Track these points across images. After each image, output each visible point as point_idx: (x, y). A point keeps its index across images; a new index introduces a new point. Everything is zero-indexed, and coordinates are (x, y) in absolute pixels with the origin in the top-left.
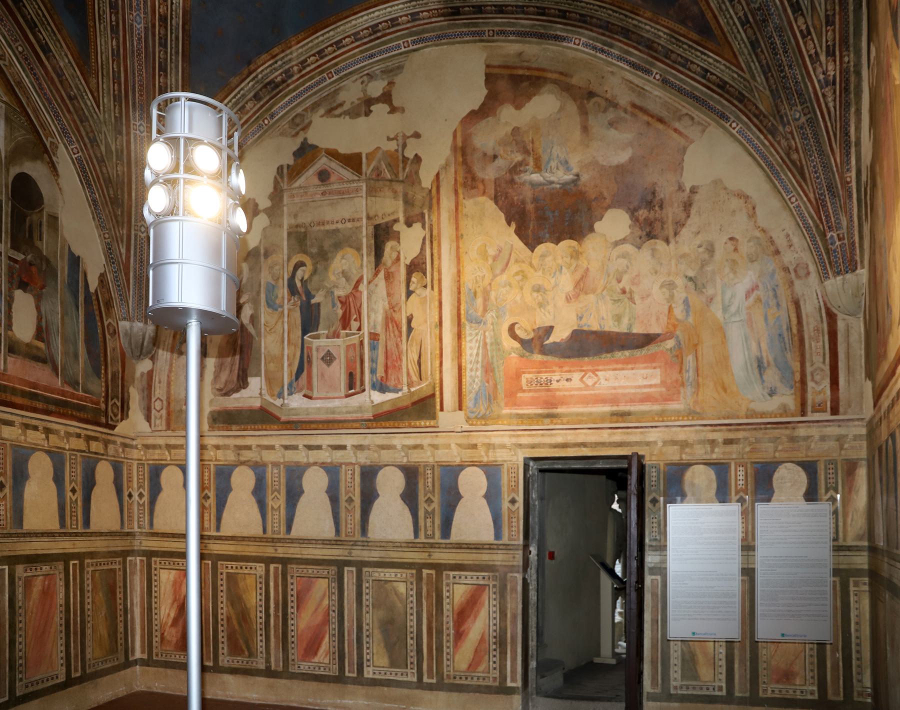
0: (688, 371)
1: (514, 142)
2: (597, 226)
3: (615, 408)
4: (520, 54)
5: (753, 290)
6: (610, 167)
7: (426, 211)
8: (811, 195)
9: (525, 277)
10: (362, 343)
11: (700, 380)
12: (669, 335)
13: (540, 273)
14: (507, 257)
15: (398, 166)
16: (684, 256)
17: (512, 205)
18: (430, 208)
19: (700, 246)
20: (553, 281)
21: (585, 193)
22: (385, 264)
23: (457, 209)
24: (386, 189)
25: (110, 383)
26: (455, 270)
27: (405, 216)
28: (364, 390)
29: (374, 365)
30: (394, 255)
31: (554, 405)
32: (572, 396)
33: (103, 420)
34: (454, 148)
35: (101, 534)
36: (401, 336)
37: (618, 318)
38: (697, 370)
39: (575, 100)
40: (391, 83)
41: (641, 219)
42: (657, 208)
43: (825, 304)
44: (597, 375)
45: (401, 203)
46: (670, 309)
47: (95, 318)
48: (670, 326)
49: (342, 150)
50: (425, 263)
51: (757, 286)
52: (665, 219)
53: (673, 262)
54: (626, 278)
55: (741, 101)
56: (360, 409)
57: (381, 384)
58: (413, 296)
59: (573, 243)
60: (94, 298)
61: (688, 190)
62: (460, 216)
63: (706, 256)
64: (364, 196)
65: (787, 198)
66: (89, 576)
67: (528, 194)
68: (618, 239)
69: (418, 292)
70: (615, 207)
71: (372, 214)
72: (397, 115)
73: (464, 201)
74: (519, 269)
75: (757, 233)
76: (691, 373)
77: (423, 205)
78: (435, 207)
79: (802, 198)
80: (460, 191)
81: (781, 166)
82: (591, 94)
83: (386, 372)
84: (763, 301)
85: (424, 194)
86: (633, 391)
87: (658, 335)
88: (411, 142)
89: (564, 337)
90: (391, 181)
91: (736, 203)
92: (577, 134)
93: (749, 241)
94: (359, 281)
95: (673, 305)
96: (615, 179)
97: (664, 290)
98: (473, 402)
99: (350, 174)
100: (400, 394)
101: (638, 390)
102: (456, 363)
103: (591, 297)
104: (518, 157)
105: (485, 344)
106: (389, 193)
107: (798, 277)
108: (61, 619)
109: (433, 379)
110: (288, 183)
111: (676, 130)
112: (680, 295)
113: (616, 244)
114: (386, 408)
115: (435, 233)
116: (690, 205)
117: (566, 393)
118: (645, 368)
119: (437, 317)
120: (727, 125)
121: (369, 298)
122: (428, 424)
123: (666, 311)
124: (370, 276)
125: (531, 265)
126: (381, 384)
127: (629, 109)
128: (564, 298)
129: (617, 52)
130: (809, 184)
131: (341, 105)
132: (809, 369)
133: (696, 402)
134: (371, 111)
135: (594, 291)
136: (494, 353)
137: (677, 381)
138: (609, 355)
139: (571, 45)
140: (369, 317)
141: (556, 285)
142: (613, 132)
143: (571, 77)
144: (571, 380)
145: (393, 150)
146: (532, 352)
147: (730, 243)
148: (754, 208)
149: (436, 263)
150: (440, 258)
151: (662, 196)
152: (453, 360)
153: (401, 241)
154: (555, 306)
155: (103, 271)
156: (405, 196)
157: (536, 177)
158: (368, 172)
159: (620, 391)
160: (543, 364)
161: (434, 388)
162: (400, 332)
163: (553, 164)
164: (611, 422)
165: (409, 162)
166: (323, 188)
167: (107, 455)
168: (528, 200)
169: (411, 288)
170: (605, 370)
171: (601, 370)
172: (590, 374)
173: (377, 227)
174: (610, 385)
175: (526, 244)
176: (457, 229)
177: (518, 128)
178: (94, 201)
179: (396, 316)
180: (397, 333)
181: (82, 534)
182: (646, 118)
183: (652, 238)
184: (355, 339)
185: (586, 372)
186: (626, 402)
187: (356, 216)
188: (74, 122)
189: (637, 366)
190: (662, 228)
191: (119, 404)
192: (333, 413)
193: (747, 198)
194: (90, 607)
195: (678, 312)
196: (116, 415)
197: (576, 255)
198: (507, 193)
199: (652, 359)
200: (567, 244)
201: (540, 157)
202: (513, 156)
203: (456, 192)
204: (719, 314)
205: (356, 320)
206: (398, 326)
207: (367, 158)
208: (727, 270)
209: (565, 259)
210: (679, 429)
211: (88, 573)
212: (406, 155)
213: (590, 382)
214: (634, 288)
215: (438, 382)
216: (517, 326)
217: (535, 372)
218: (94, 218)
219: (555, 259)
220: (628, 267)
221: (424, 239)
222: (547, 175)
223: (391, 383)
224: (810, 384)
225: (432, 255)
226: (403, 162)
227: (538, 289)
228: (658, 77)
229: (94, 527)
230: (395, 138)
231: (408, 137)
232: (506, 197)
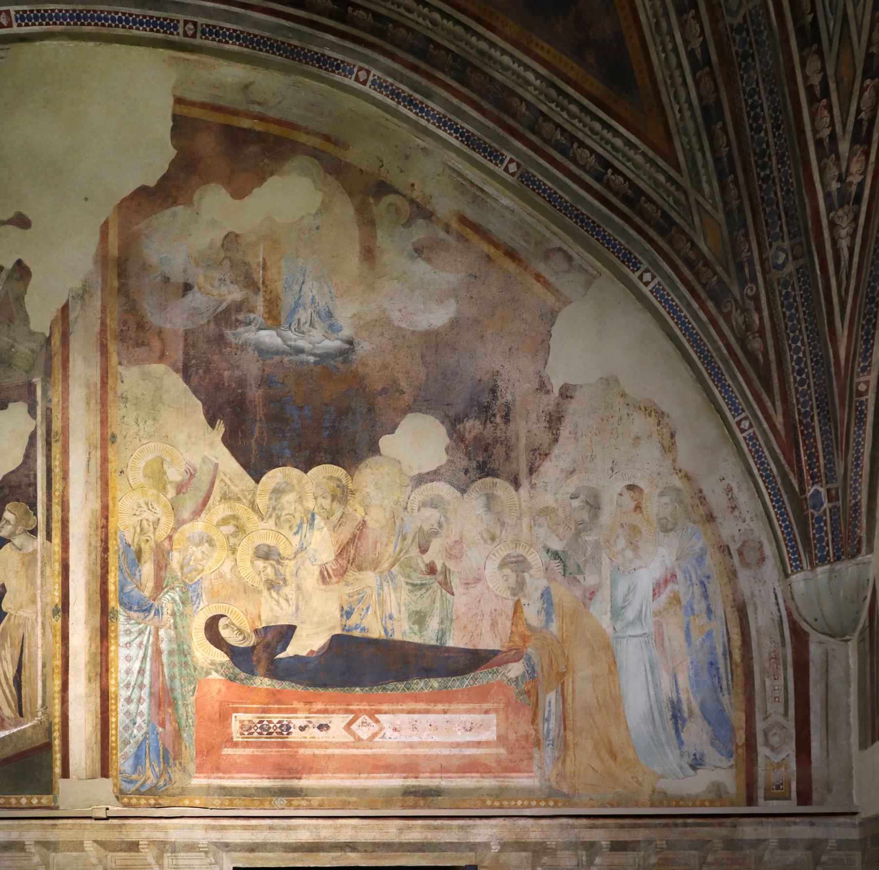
0: (547, 720)
1: (227, 262)
2: (385, 442)
3: (411, 782)
4: (246, 87)
5: (666, 582)
6: (414, 332)
8: (779, 420)
9: (240, 530)
11: (570, 736)
12: (515, 654)
13: (271, 523)
14: (205, 487)
16: (545, 512)
17: (218, 386)
18: (48, 374)
19: (574, 497)
20: (296, 540)
21: (363, 378)
26: (96, 505)
31: (296, 774)
32: (329, 757)
34: (103, 259)
37: (420, 619)
38: (564, 719)
39: (350, 195)
41: (469, 437)
42: (498, 419)
43: (789, 615)
44: (377, 721)
46: (517, 607)
48: (516, 638)
51: (674, 576)
52: (513, 441)
53: (525, 521)
54: (436, 545)
55: (662, 233)
59: (338, 472)
61: (556, 392)
62: (111, 396)
63: (585, 515)
65: (733, 422)
67: (252, 368)
68: (425, 470)
70: (420, 411)
73: (120, 369)
74: (229, 513)
75: (677, 482)
76: (553, 724)
78: (58, 374)
79: (760, 424)
81: (725, 362)
82: (383, 188)
84: (684, 603)
86: (446, 752)
87: (494, 653)
89: (315, 649)
91: (640, 423)
92: (353, 261)
93: (662, 494)
95: (523, 601)
96: (423, 356)
97: (507, 571)
98: (131, 761)
101: (456, 751)
102: (96, 686)
103: (370, 578)
104: (235, 294)
105: (158, 652)
107: (745, 564)
109: (49, 716)
111: (538, 277)
112: (536, 582)
113: (421, 480)
115: (56, 425)
116: (560, 419)
117: (318, 752)
118: (468, 711)
119: (57, 594)
120: (634, 277)
122: (35, 801)
123: (510, 612)
125: (253, 506)
127: (454, 225)
128: (317, 572)
129: (438, 109)
130: (777, 397)
132: (760, 725)
133: (561, 776)
135: (375, 565)
136: (176, 670)
137: (527, 737)
138: (401, 686)
139: (350, 82)
141: (302, 549)
142: (421, 267)
143: (346, 147)
144: (327, 727)
146: (252, 672)
147: (627, 495)
148: (672, 436)
149: (57, 486)
150: (65, 477)
151: (509, 397)
152: (90, 680)
154: (299, 588)
157: (268, 337)
159: (421, 751)
160: (274, 696)
161: (49, 731)
163: (304, 315)
164: (404, 807)
168: (252, 382)
170: (393, 712)
171: (386, 713)
172: (364, 718)
174: (403, 739)
175: (245, 466)
176: (104, 422)
177: (237, 236)
182: (486, 247)
183: (487, 475)
185: (357, 714)
186: (433, 771)
189: (454, 706)
190: (508, 458)
193: (662, 415)
195: (532, 613)
197: (342, 495)
198: (209, 362)
199: (481, 695)
200: (323, 472)
201: (278, 298)
202: (224, 290)
203: (104, 350)
204: (606, 622)
208: (622, 543)
209: (321, 500)
210: (531, 821)
213: (364, 733)
214: (451, 565)
215: (57, 720)
216: (222, 622)
217: (256, 711)
219: (300, 500)
220: (440, 525)
222: (290, 334)
224: (762, 751)
225: (49, 470)
227: (266, 554)
228: (513, 168)
232: (207, 371)
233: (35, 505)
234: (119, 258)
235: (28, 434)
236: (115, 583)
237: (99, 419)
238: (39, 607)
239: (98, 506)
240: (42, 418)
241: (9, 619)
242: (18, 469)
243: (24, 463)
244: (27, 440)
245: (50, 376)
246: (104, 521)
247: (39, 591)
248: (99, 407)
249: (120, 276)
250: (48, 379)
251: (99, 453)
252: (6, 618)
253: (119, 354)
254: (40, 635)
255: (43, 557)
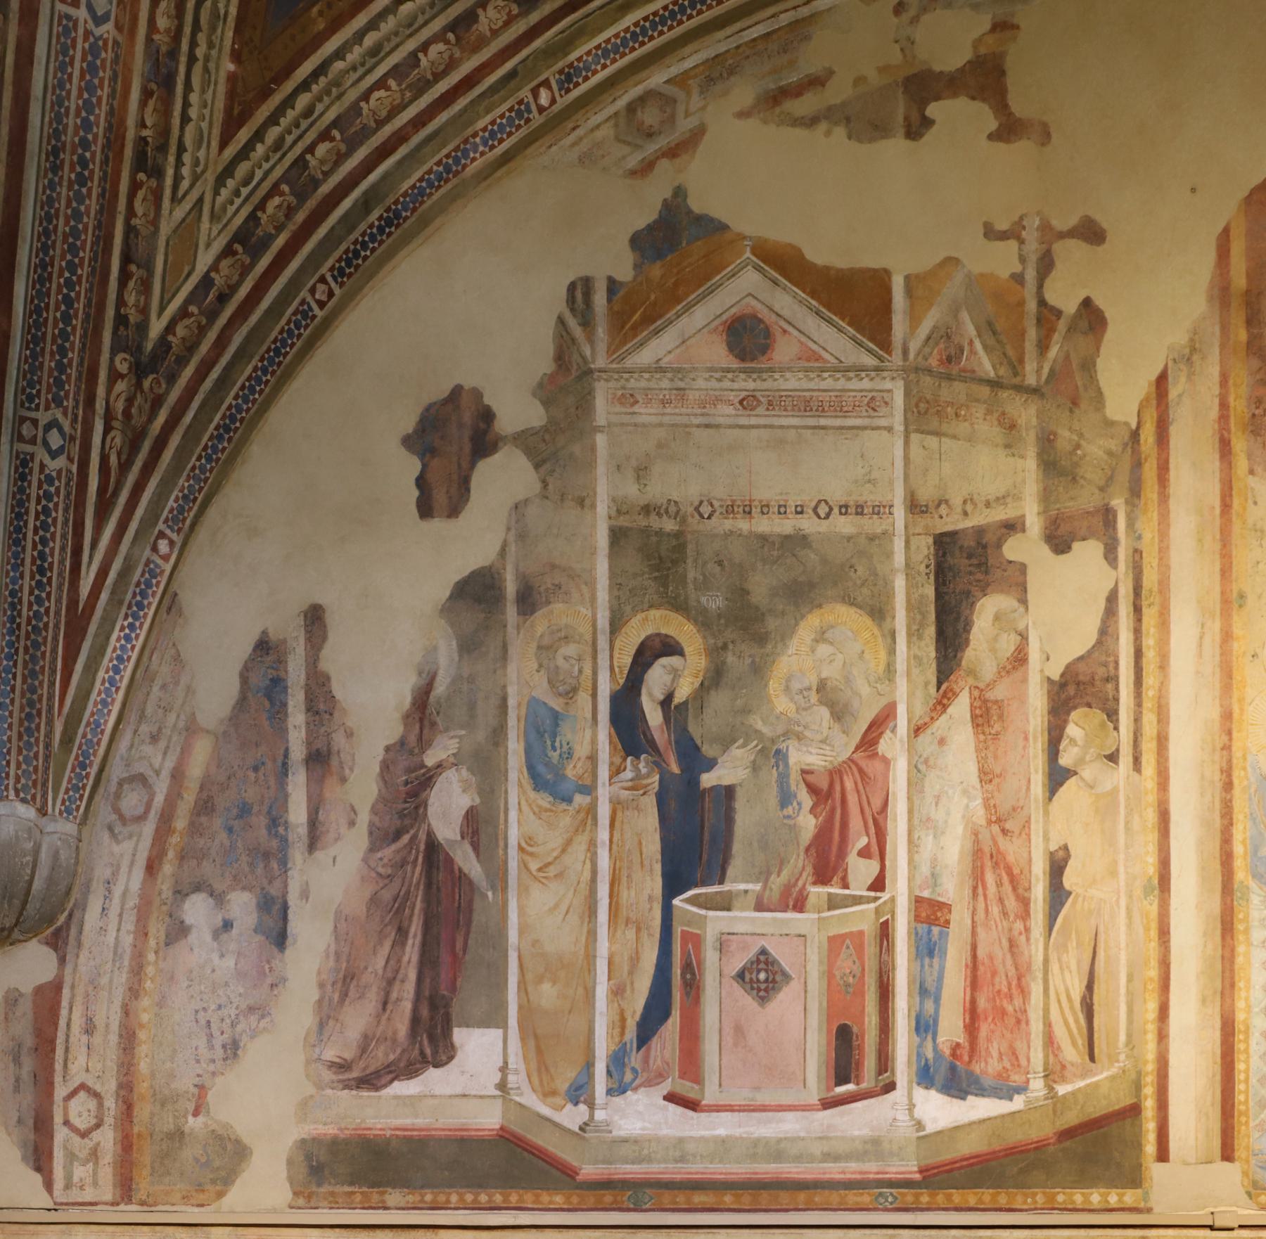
7: (1118, 503)
10: (885, 932)
15: (1023, 334)
18: (1135, 491)
22: (972, 672)
23: (1226, 506)
24: (979, 411)
26: (1213, 712)
27: (1044, 512)
28: (890, 1087)
29: (929, 1006)
30: (1008, 644)
34: (1222, 293)
36: (1025, 914)
40: (1003, 27)
45: (1030, 464)
49: (819, 255)
50: (1113, 679)
56: (873, 1148)
57: (953, 1068)
58: (1070, 788)
62: (1237, 527)
64: (899, 428)
69: (1087, 773)
71: (926, 494)
72: (1023, 148)
73: (1251, 481)
77: (1110, 479)
80: (1239, 444)
83: (971, 1028)
85: (1114, 445)
88: (1071, 254)
90: (995, 384)
94: (881, 722)
99: (850, 345)
100: (1018, 1103)
106: (987, 428)
110: (610, 352)
114: (969, 1146)
115: (1150, 579)
121: (915, 785)
124: (920, 710)
126: (953, 1068)
131: (816, 82)
134: (927, 123)
140: (912, 844)
145: (1004, 274)
149: (1150, 680)
150: (1163, 666)
153: (1030, 596)
156: (1047, 442)
158: (914, 346)
162: (1025, 903)
165: (1062, 326)
166: (747, 384)
169: (1065, 760)
173: (944, 543)
176: (1226, 572)
179: (1011, 849)
180: (1012, 904)
184: (861, 919)
187: (869, 496)
192: (779, 1156)
205: (864, 853)
206: (1016, 881)
207: (909, 291)
212: (1051, 298)
221: (1112, 598)
223: (989, 1066)
225: (1138, 654)
226: (1040, 321)
230: (1014, 234)
231: (1062, 235)
233: (1116, 712)
234: (1248, 292)
235: (1105, 594)
236: (1244, 842)
237: (1218, 567)
238: (1122, 883)
239: (1215, 713)
240: (1127, 567)
241: (1074, 903)
242: (1090, 652)
243: (1099, 643)
244: (1102, 604)
245: (1139, 496)
246: (1225, 738)
247: (1122, 856)
248: (1218, 546)
249: (1249, 322)
250: (1136, 501)
251: (1217, 625)
252: (1070, 900)
253: (1250, 456)
254: (1123, 928)
255: (1128, 799)
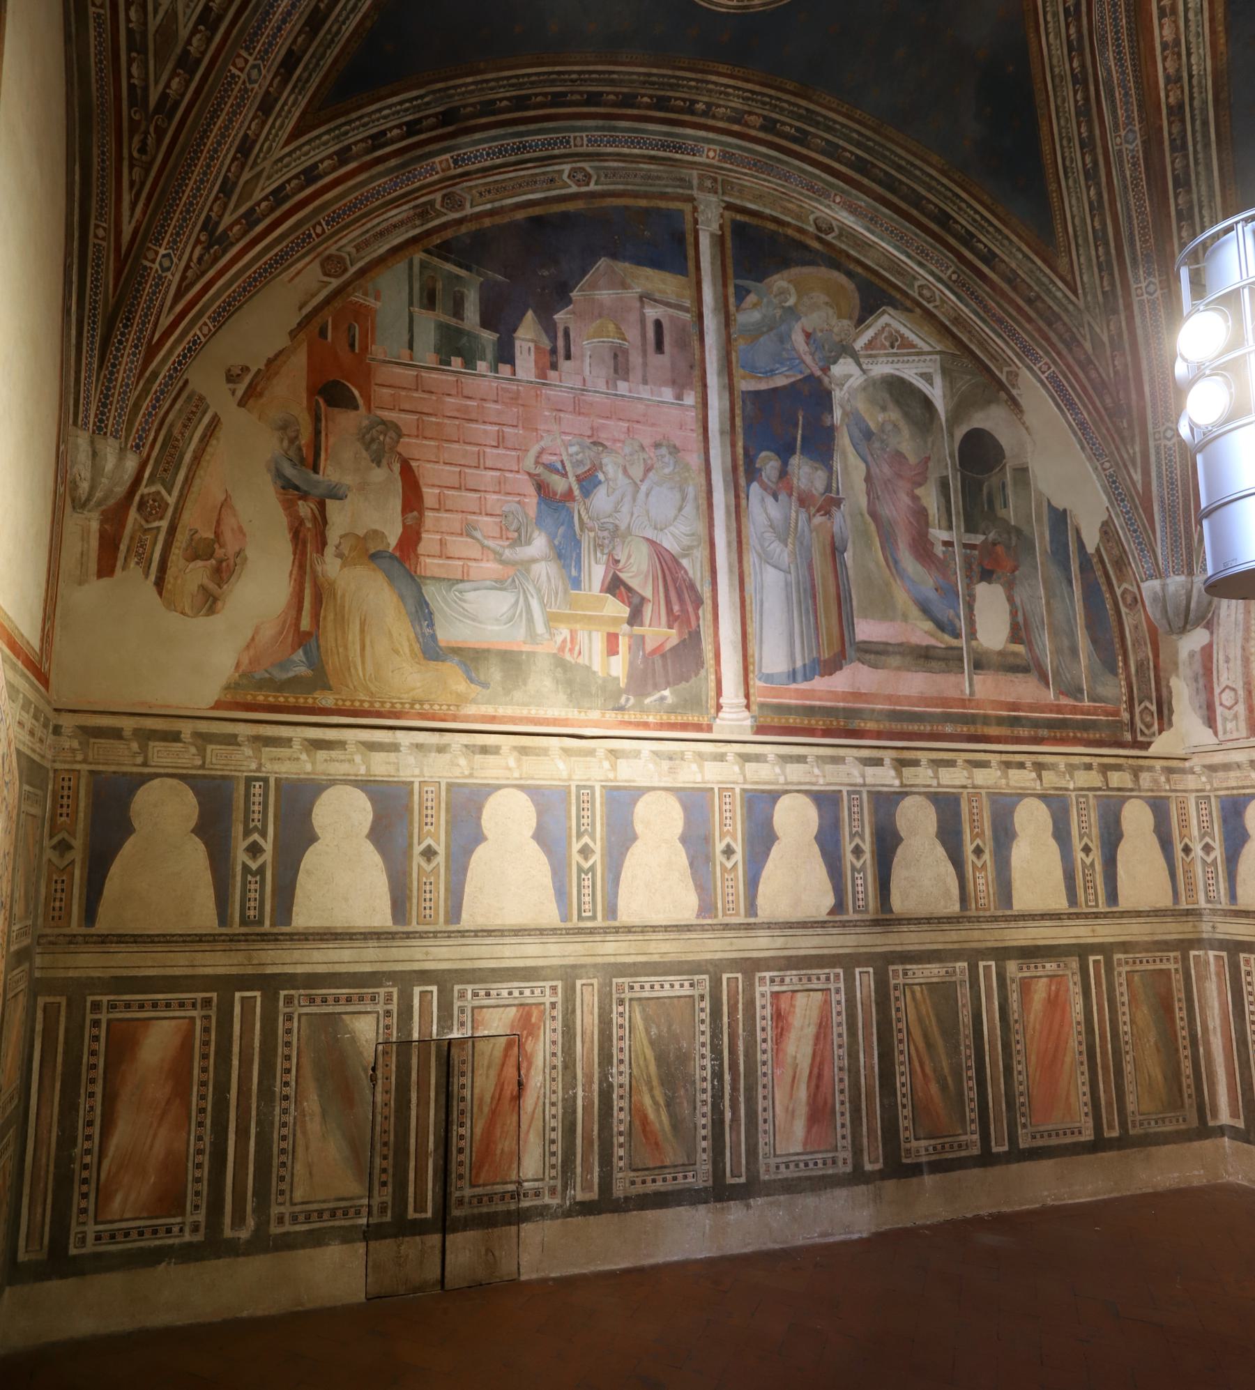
25: (1134, 679)
33: (1128, 737)
35: (1138, 914)
47: (1100, 589)
60: (1095, 560)
66: (1123, 980)
108: (1080, 1043)
155: (1105, 517)
167: (1140, 790)
178: (1082, 425)
181: (1105, 915)
188: (1040, 330)
191: (1154, 708)
194: (1127, 1028)
196: (1149, 726)
211: (1120, 974)
218: (1083, 448)
229: (1124, 904)
